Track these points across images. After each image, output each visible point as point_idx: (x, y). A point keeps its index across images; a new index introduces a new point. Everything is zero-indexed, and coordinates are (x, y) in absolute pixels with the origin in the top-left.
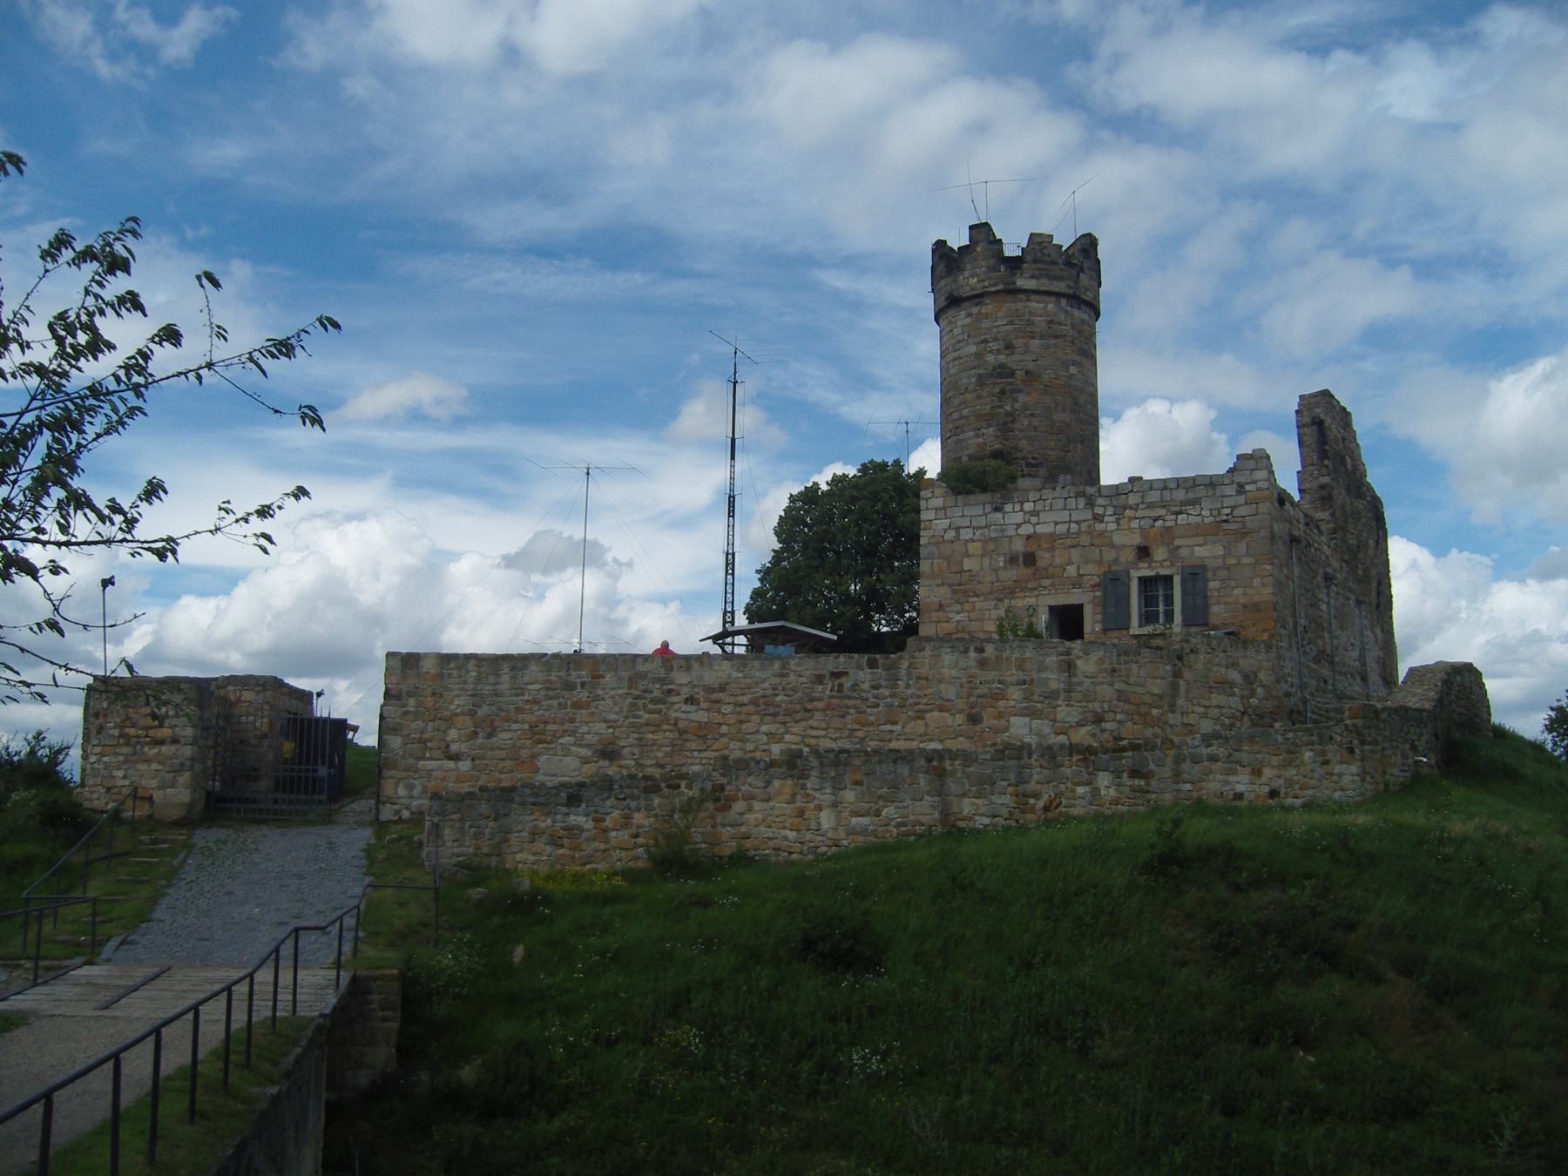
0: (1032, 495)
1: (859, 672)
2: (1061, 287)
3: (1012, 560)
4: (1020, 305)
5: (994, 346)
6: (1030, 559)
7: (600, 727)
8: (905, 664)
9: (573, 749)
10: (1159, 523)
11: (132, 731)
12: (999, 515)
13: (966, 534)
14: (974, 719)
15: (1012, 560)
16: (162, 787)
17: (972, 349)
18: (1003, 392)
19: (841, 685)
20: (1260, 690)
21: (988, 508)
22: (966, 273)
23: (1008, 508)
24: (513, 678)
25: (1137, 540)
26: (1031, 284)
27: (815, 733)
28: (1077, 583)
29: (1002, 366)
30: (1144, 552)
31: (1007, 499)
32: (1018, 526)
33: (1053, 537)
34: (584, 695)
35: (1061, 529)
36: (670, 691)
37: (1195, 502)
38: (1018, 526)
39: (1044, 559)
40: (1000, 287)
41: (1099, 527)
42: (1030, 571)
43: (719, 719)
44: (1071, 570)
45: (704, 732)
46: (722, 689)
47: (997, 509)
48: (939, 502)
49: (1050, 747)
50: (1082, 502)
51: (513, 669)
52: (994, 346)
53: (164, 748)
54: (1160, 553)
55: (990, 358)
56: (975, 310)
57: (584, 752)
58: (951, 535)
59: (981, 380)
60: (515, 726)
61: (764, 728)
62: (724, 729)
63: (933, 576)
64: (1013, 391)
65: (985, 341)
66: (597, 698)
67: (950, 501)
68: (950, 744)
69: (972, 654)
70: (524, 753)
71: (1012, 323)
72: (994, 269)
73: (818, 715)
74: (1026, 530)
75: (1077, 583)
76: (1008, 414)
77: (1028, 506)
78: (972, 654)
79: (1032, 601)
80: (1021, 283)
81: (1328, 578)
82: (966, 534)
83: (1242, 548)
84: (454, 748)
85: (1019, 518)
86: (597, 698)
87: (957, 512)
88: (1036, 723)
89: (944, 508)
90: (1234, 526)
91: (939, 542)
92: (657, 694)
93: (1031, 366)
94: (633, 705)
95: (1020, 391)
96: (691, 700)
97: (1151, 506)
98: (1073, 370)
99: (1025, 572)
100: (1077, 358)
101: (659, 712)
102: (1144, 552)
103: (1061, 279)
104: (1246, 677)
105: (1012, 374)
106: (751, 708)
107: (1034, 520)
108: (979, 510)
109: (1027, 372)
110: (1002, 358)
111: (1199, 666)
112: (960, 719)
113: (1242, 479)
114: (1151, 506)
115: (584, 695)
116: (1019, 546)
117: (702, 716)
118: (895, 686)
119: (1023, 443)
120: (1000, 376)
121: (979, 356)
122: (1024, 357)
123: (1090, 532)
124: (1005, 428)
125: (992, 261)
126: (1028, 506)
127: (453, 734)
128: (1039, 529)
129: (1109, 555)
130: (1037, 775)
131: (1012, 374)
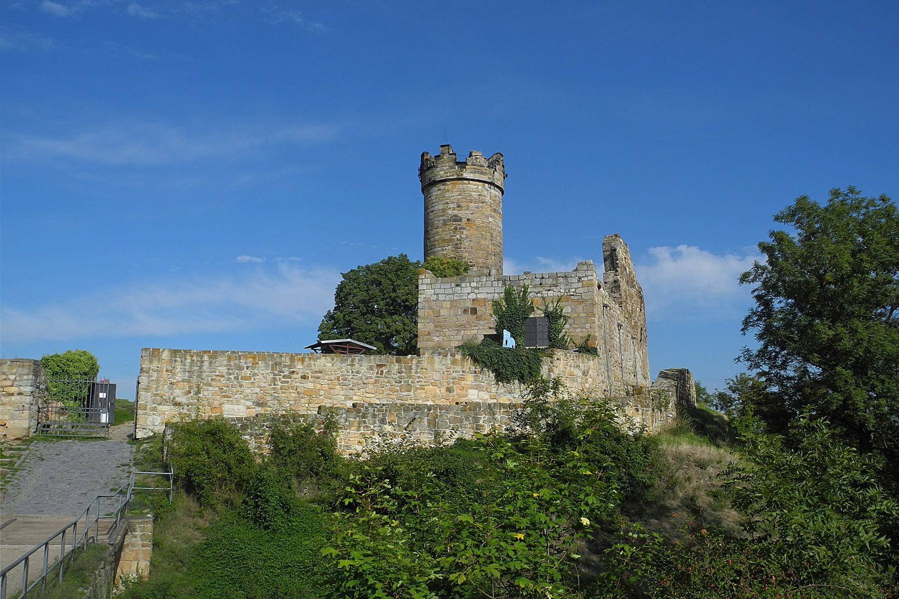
1: (393, 365)
2: (485, 178)
4: (465, 186)
6: (474, 311)
7: (257, 390)
8: (414, 362)
9: (242, 401)
10: (539, 295)
12: (459, 288)
13: (441, 297)
14: (449, 390)
15: (465, 311)
16: (12, 417)
18: (456, 229)
19: (382, 372)
20: (590, 380)
21: (453, 285)
22: (438, 169)
23: (463, 285)
24: (211, 363)
26: (471, 176)
27: (368, 395)
29: (456, 216)
31: (463, 280)
32: (469, 294)
34: (248, 373)
36: (293, 372)
38: (469, 294)
40: (455, 177)
42: (475, 316)
43: (319, 386)
45: (310, 394)
46: (321, 372)
47: (457, 285)
48: (428, 281)
49: (489, 405)
51: (210, 357)
53: (13, 398)
57: (250, 403)
60: (210, 388)
61: (343, 392)
62: (322, 392)
63: (424, 318)
64: (460, 228)
65: (447, 203)
66: (255, 374)
68: (437, 402)
69: (449, 357)
70: (216, 403)
71: (460, 195)
72: (452, 168)
73: (371, 386)
76: (458, 240)
77: (474, 284)
78: (449, 357)
79: (475, 332)
80: (465, 175)
81: (620, 326)
82: (441, 297)
83: (580, 308)
84: (178, 400)
85: (469, 290)
86: (255, 374)
88: (481, 393)
89: (431, 284)
90: (576, 298)
91: (427, 300)
92: (287, 373)
93: (470, 217)
94: (274, 379)
95: (464, 229)
96: (304, 377)
98: (490, 219)
99: (469, 316)
100: (493, 214)
101: (288, 382)
103: (485, 174)
104: (584, 373)
106: (337, 382)
107: (476, 291)
108: (448, 286)
109: (468, 220)
110: (456, 212)
111: (561, 366)
112: (443, 390)
113: (580, 275)
115: (248, 373)
116: (469, 305)
117: (310, 386)
118: (410, 372)
119: (466, 254)
120: (454, 221)
122: (467, 212)
126: (474, 284)
127: (177, 392)
130: (483, 419)
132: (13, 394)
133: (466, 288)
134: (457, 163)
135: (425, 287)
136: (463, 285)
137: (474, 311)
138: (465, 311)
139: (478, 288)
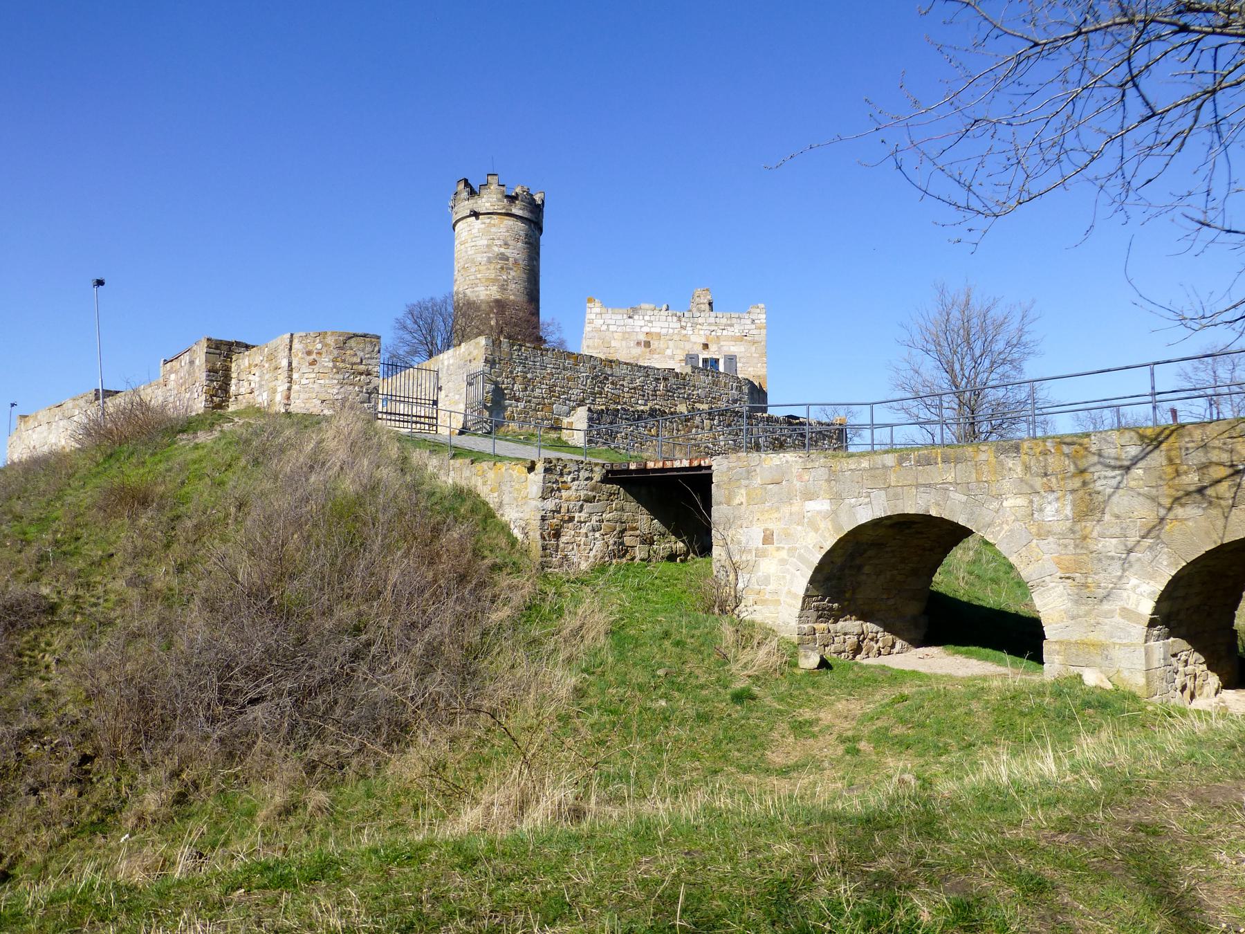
0: (649, 313)
3: (638, 344)
5: (498, 242)
6: (647, 344)
11: (342, 365)
13: (612, 328)
17: (485, 242)
18: (502, 268)
25: (704, 341)
28: (672, 357)
30: (706, 346)
33: (659, 335)
35: (664, 331)
37: (732, 325)
39: (654, 344)
41: (684, 332)
44: (669, 352)
48: (597, 310)
50: (675, 319)
52: (498, 242)
54: (713, 347)
55: (496, 249)
56: (488, 221)
58: (604, 327)
59: (489, 261)
67: (604, 310)
74: (646, 329)
75: (672, 357)
77: (647, 318)
82: (612, 328)
85: (642, 323)
87: (608, 316)
97: (710, 324)
102: (706, 346)
105: (507, 259)
108: (620, 317)
110: (502, 250)
114: (710, 324)
116: (642, 338)
121: (488, 246)
123: (679, 334)
124: (503, 288)
125: (500, 196)
126: (647, 318)
128: (653, 330)
129: (688, 346)
131: (507, 259)
132: (361, 374)
133: (638, 321)
134: (507, 197)
135: (593, 316)
136: (636, 317)
137: (647, 344)
138: (638, 344)
139: (651, 322)
